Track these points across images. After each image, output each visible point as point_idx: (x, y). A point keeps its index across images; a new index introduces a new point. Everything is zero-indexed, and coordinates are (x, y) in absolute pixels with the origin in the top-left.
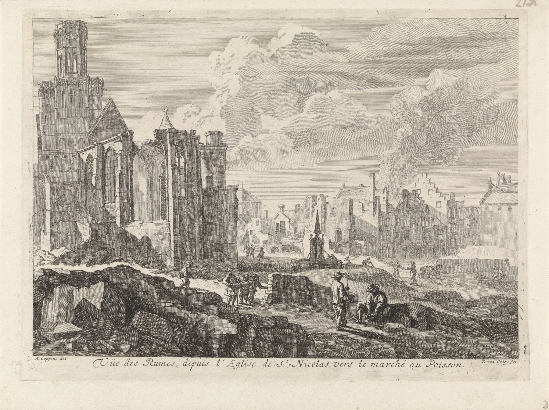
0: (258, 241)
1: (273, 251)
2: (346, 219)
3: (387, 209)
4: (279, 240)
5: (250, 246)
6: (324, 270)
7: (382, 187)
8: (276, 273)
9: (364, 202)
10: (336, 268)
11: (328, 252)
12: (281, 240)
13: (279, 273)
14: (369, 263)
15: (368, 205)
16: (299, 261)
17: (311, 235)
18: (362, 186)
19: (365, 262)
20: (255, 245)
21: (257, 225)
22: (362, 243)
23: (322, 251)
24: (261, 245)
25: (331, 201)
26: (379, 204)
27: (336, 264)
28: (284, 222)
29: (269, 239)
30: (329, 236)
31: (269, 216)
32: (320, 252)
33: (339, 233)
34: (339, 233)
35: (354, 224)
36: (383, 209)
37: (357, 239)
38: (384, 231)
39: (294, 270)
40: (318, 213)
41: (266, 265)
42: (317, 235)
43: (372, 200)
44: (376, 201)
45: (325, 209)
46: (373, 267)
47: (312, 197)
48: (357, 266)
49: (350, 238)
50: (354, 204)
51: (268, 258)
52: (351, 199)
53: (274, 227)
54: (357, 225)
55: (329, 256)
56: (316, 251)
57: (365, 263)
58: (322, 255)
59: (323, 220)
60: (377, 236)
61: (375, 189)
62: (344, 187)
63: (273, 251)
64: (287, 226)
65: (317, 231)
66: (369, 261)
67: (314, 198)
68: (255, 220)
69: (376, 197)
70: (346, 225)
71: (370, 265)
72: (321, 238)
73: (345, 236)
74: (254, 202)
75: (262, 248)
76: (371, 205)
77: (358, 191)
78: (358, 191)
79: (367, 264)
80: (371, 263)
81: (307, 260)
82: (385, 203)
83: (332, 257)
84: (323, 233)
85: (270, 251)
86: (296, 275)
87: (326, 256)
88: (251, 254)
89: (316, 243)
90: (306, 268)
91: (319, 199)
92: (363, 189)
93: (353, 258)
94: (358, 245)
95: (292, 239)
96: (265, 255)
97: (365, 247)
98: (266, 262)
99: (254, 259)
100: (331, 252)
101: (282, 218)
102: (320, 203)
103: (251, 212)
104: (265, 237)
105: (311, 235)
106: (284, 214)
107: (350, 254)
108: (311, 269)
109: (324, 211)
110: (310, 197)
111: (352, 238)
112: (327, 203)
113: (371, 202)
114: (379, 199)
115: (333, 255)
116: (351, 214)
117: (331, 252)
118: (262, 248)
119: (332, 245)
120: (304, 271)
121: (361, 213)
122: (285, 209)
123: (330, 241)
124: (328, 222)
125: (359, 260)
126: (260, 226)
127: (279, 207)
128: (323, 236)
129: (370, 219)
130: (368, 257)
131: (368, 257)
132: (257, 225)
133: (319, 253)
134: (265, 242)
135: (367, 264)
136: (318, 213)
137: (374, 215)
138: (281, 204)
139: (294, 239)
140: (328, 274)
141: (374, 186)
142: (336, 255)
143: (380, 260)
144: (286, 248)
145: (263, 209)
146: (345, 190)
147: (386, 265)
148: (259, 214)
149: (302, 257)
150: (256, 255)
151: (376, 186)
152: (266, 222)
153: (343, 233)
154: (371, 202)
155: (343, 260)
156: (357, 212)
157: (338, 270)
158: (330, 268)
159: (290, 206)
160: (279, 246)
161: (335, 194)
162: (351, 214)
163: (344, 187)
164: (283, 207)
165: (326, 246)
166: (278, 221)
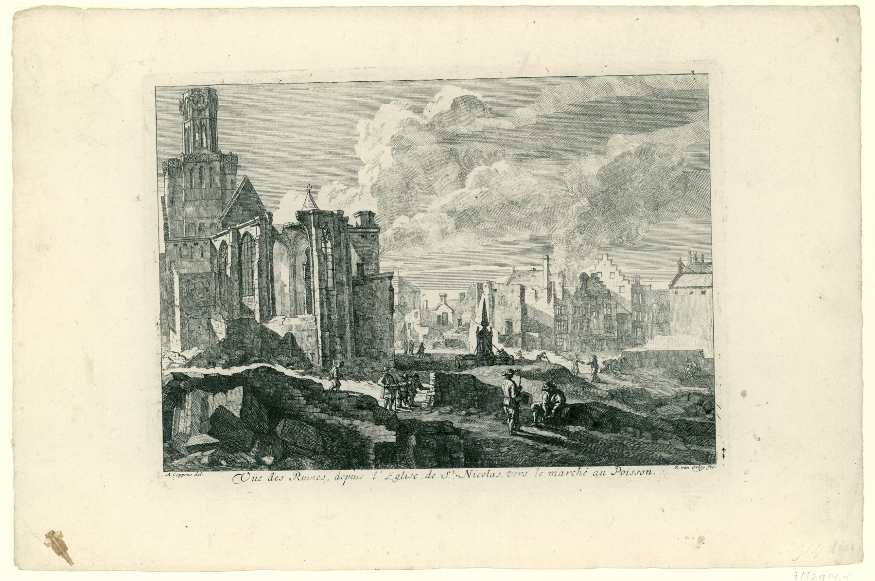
0: (417, 336)
1: (434, 346)
2: (517, 308)
4: (441, 334)
7: (558, 270)
9: (536, 288)
10: (507, 364)
11: (497, 346)
16: (465, 358)
17: (478, 328)
18: (534, 270)
19: (539, 357)
20: (414, 340)
22: (536, 335)
23: (490, 345)
24: (421, 340)
25: (500, 288)
27: (506, 359)
29: (430, 333)
30: (498, 328)
33: (509, 324)
34: (509, 324)
35: (526, 314)
36: (559, 296)
38: (561, 321)
41: (427, 363)
42: (485, 328)
43: (546, 286)
44: (550, 288)
45: (493, 297)
48: (530, 362)
51: (428, 355)
53: (435, 320)
54: (530, 315)
58: (491, 349)
60: (552, 327)
61: (549, 274)
62: (514, 271)
63: (434, 346)
64: (450, 318)
65: (485, 323)
67: (480, 286)
68: (413, 312)
70: (516, 316)
73: (517, 329)
75: (422, 344)
82: (561, 289)
83: (502, 352)
84: (490, 325)
86: (461, 373)
87: (495, 351)
89: (484, 336)
92: (536, 274)
94: (532, 338)
96: (425, 351)
98: (427, 359)
100: (501, 346)
101: (444, 309)
102: (486, 290)
104: (426, 331)
105: (478, 328)
107: (522, 348)
111: (525, 329)
112: (495, 290)
115: (503, 350)
116: (522, 301)
117: (501, 346)
118: (422, 344)
119: (502, 339)
123: (499, 333)
124: (496, 312)
125: (532, 355)
126: (419, 318)
129: (544, 308)
133: (487, 348)
134: (425, 336)
137: (549, 303)
138: (443, 292)
140: (498, 372)
141: (548, 270)
142: (506, 349)
143: (557, 354)
144: (450, 343)
145: (423, 299)
146: (515, 275)
149: (467, 353)
150: (415, 352)
152: (426, 313)
155: (514, 355)
156: (529, 300)
158: (500, 364)
159: (453, 295)
160: (441, 341)
161: (505, 279)
162: (522, 301)
163: (514, 271)
164: (445, 296)
165: (495, 340)
166: (439, 312)
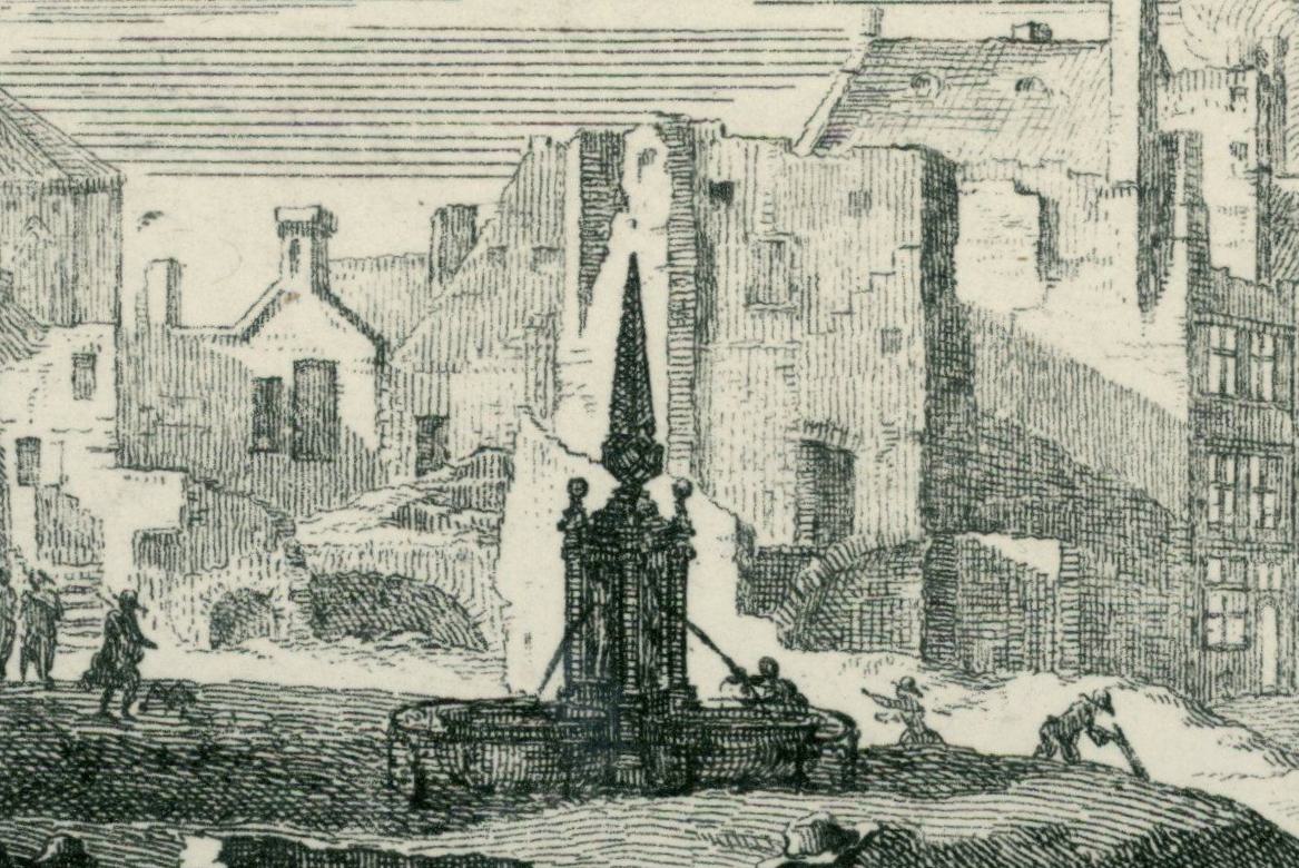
0: (89, 545)
1: (225, 627)
2: (890, 341)
3: (1264, 249)
4: (282, 528)
5: (19, 583)
6: (690, 803)
7: (1224, 46)
8: (255, 829)
9: (1051, 182)
10: (800, 783)
11: (726, 640)
12: (304, 535)
13: (282, 828)
14: (1102, 738)
15: (1093, 213)
16: (466, 723)
17: (578, 488)
18: (1040, 36)
19: (1061, 734)
20: (61, 576)
21: (84, 392)
22: (1042, 556)
23: (671, 628)
24: (119, 571)
25: (763, 179)
26: (1196, 204)
27: (796, 746)
28: (331, 369)
29: (191, 518)
30: (735, 492)
31: (194, 312)
32: (655, 637)
33: (828, 461)
34: (828, 461)
35: (962, 385)
36: (1234, 247)
37: (996, 527)
38: (1239, 449)
39: (418, 801)
40: (633, 285)
41: (164, 759)
42: (630, 490)
43: (1125, 169)
44: (1159, 186)
45: (704, 249)
46: (1139, 772)
47: (586, 138)
48: (989, 773)
49: (928, 511)
50: (966, 206)
51: (174, 694)
52: (934, 160)
53: (238, 414)
54: (994, 394)
55: (738, 675)
56: (616, 632)
57: (1068, 742)
58: (677, 662)
59: (683, 345)
60: (1171, 497)
61: (1155, 70)
62: (879, 43)
63: (225, 627)
64: (357, 407)
65: (631, 448)
66: (1103, 720)
67: (603, 155)
68: (60, 346)
69: (1169, 142)
70: (884, 399)
71: (1111, 755)
72: (667, 510)
73: (886, 502)
74: (56, 188)
75: (129, 604)
76: (1125, 209)
77: (1004, 84)
78: (1004, 84)
79: (1086, 748)
80: (1120, 738)
81: (535, 709)
82: (1244, 195)
83: (765, 687)
84: (677, 468)
85: (203, 625)
86: (435, 847)
87: (707, 677)
88: (29, 655)
89: (623, 556)
90: (525, 787)
91: (644, 158)
92: (1051, 69)
93: (954, 693)
94: (1007, 581)
95: (400, 519)
96: (153, 667)
97: (1067, 595)
98: (161, 726)
99: (55, 707)
100: (754, 641)
101: (306, 328)
102: (652, 189)
103: (24, 278)
104: (160, 501)
105: (578, 488)
106: (323, 290)
107: (927, 655)
108: (569, 794)
109: (688, 260)
110: (562, 134)
111: (952, 508)
112: (723, 191)
113: (1120, 188)
114: (1195, 152)
115: (770, 670)
116: (938, 279)
117: (754, 641)
118: (129, 604)
119: (763, 582)
120: (511, 812)
121: (1028, 286)
122: (336, 246)
123: (743, 534)
124: (725, 361)
125: (1004, 719)
126: (104, 400)
127: (284, 229)
128: (682, 494)
129: (1108, 344)
130: (1094, 685)
131: (1094, 685)
132: (84, 392)
133: (642, 652)
134: (152, 546)
135: (1086, 748)
136: (633, 285)
137: (1146, 301)
138: (300, 198)
139: (422, 523)
140: (731, 842)
141: (1149, 40)
142: (799, 668)
143: (1203, 713)
144: (349, 605)
145: (141, 248)
146: (879, 73)
147: (1255, 761)
148: (94, 297)
149: (485, 687)
150: (71, 664)
151: (1169, 38)
152: (160, 359)
153: (864, 465)
154: (1120, 188)
155: (862, 712)
156: (990, 275)
157: (818, 807)
158: (745, 784)
159: (383, 221)
160: (280, 582)
161: (796, 106)
162: (938, 279)
163: (879, 43)
164: (322, 224)
165: (711, 592)
166: (269, 358)
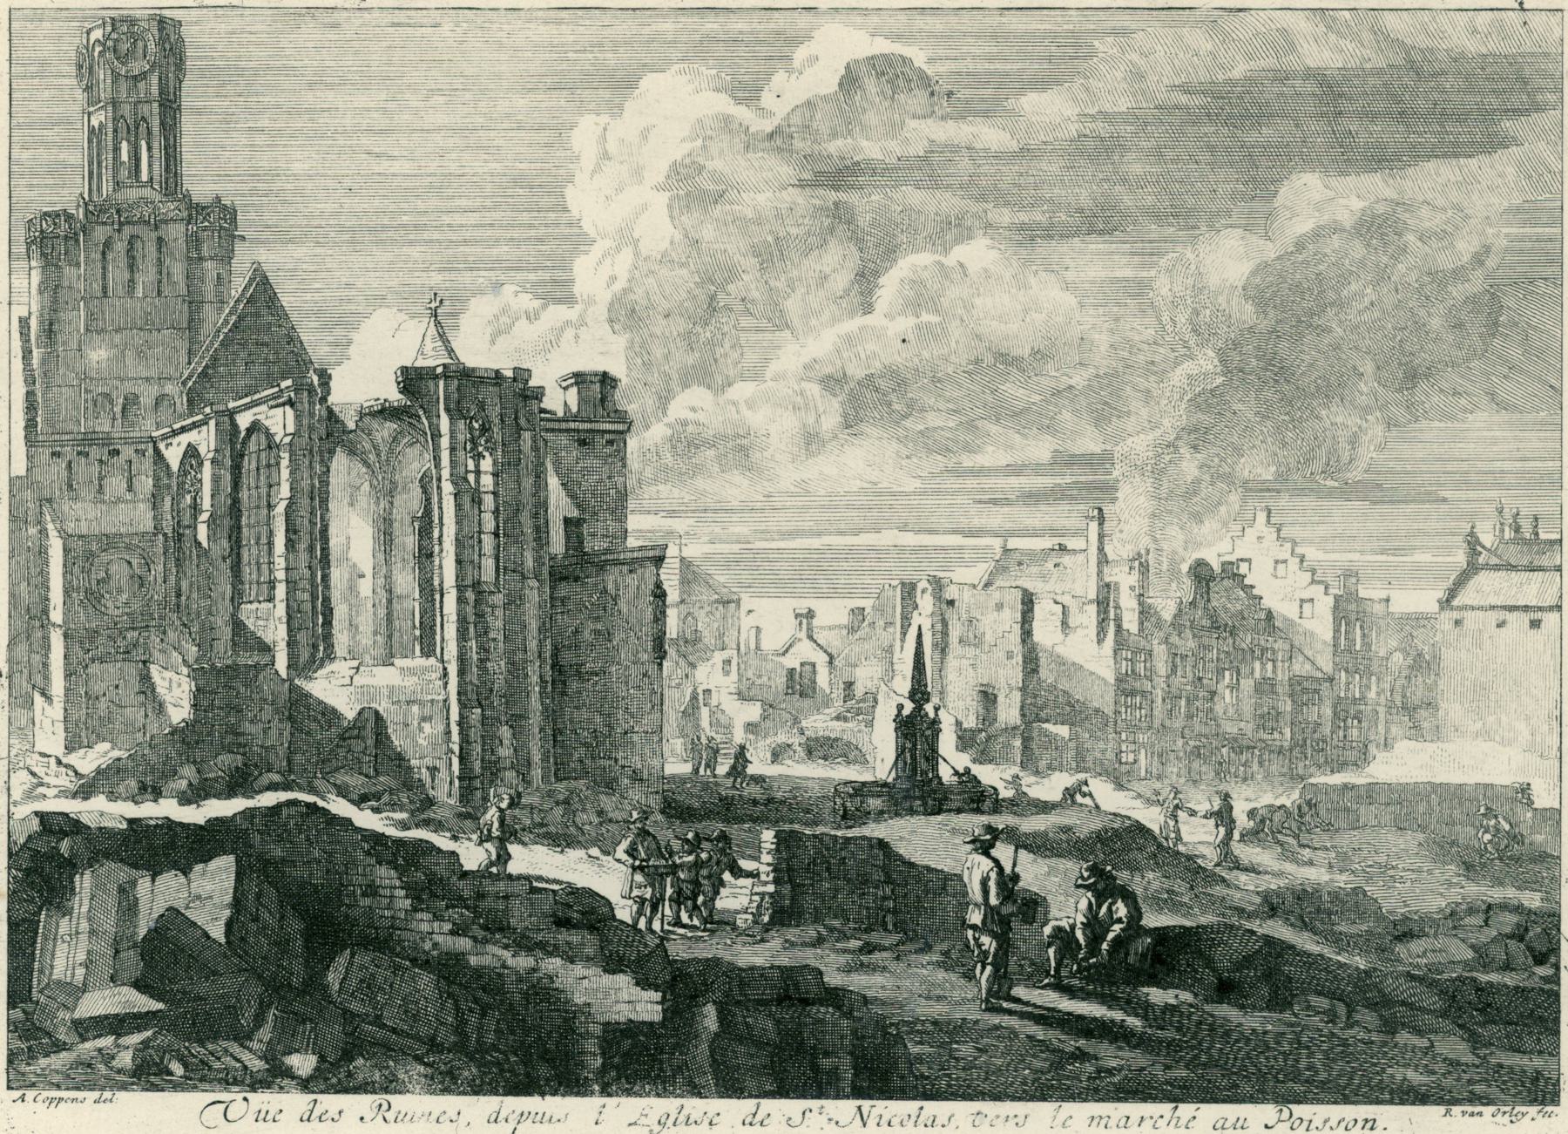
0: (728, 727)
1: (776, 756)
2: (1010, 655)
3: (1141, 623)
4: (796, 721)
5: (704, 741)
6: (940, 818)
7: (1127, 552)
8: (787, 827)
9: (1066, 599)
10: (978, 811)
11: (952, 759)
12: (804, 724)
13: (796, 827)
14: (1084, 795)
15: (1081, 611)
16: (861, 790)
17: (900, 707)
18: (1062, 548)
19: (1070, 793)
20: (719, 738)
21: (727, 673)
22: (1063, 731)
23: (933, 756)
24: (739, 736)
25: (965, 598)
26: (1117, 607)
27: (976, 797)
28: (814, 665)
29: (764, 718)
30: (955, 709)
31: (765, 645)
32: (927, 759)
33: (988, 698)
34: (988, 698)
35: (1035, 671)
36: (1131, 623)
37: (1047, 721)
38: (1133, 693)
39: (844, 817)
40: (920, 636)
41: (755, 802)
42: (919, 708)
43: (1092, 595)
44: (1104, 601)
45: (945, 623)
46: (1097, 807)
47: (903, 584)
48: (1044, 807)
49: (1023, 715)
50: (1036, 607)
51: (758, 780)
52: (1025, 591)
53: (781, 681)
54: (1046, 674)
55: (956, 773)
56: (914, 758)
57: (1072, 796)
58: (935, 768)
59: (937, 657)
60: (1109, 710)
61: (1103, 560)
62: (1006, 551)
63: (776, 756)
64: (823, 679)
65: (919, 693)
66: (1085, 789)
67: (909, 590)
68: (719, 657)
69: (1108, 585)
70: (1008, 675)
71: (1087, 801)
72: (932, 715)
73: (1009, 712)
74: (717, 601)
75: (742, 748)
76: (1093, 608)
77: (1050, 565)
78: (1050, 565)
79: (1079, 798)
80: (1091, 795)
81: (885, 785)
82: (1134, 604)
84: (935, 700)
85: (769, 755)
86: (850, 833)
87: (945, 773)
88: (707, 766)
89: (916, 731)
90: (882, 812)
91: (923, 591)
92: (1066, 560)
93: (1033, 779)
94: (1051, 739)
95: (838, 718)
96: (750, 770)
97: (1072, 745)
98: (754, 791)
99: (717, 784)
100: (962, 761)
101: (805, 651)
102: (926, 603)
103: (706, 633)
104: (753, 712)
105: (900, 707)
106: (810, 638)
107: (1023, 766)
108: (897, 815)
109: (939, 627)
110: (895, 583)
111: (1032, 714)
112: (951, 603)
113: (1091, 602)
114: (1117, 589)
115: (968, 771)
116: (1027, 634)
117: (962, 761)
118: (742, 748)
119: (965, 740)
120: (877, 821)
121: (1059, 636)
122: (815, 622)
123: (958, 723)
124: (952, 662)
126: (734, 676)
127: (797, 616)
128: (937, 709)
129: (1086, 656)
130: (1082, 776)
131: (1082, 776)
132: (727, 673)
133: (923, 765)
134: (751, 727)
135: (1079, 798)
136: (920, 636)
137: (1100, 641)
138: (803, 605)
139: (846, 719)
140: (954, 831)
141: (1101, 549)
142: (977, 770)
143: (1120, 786)
144: (819, 748)
145: (747, 622)
146: (1006, 561)
147: (1138, 803)
148: (730, 640)
150: (722, 769)
151: (1108, 549)
152: (754, 662)
153: (1001, 699)
154: (1091, 602)
155: (1000, 786)
156: (1045, 632)
157: (985, 819)
158: (959, 811)
159: (832, 613)
160: (796, 740)
162: (1027, 634)
163: (1006, 551)
164: (810, 614)
165: (947, 743)
166: (792, 661)
